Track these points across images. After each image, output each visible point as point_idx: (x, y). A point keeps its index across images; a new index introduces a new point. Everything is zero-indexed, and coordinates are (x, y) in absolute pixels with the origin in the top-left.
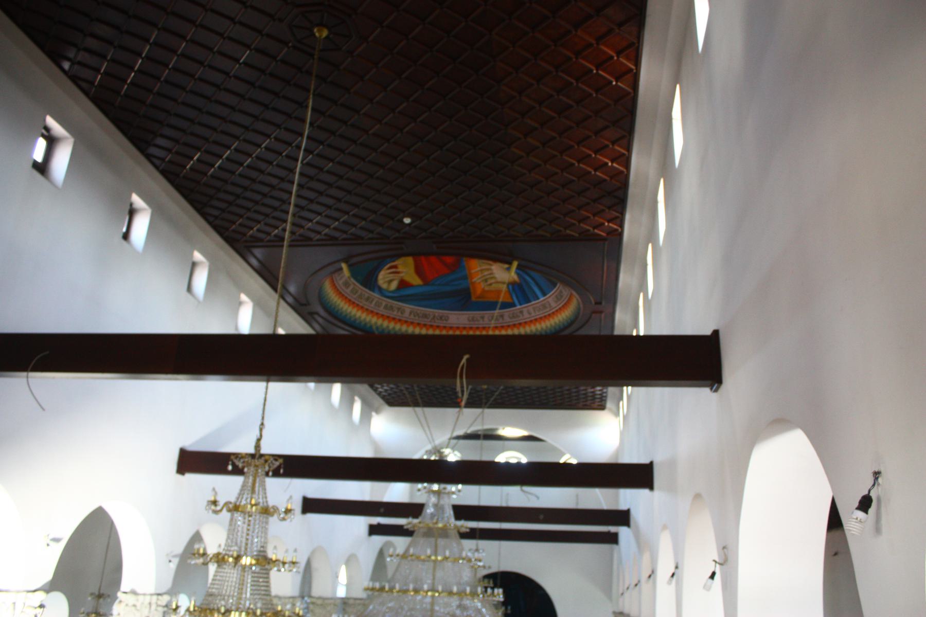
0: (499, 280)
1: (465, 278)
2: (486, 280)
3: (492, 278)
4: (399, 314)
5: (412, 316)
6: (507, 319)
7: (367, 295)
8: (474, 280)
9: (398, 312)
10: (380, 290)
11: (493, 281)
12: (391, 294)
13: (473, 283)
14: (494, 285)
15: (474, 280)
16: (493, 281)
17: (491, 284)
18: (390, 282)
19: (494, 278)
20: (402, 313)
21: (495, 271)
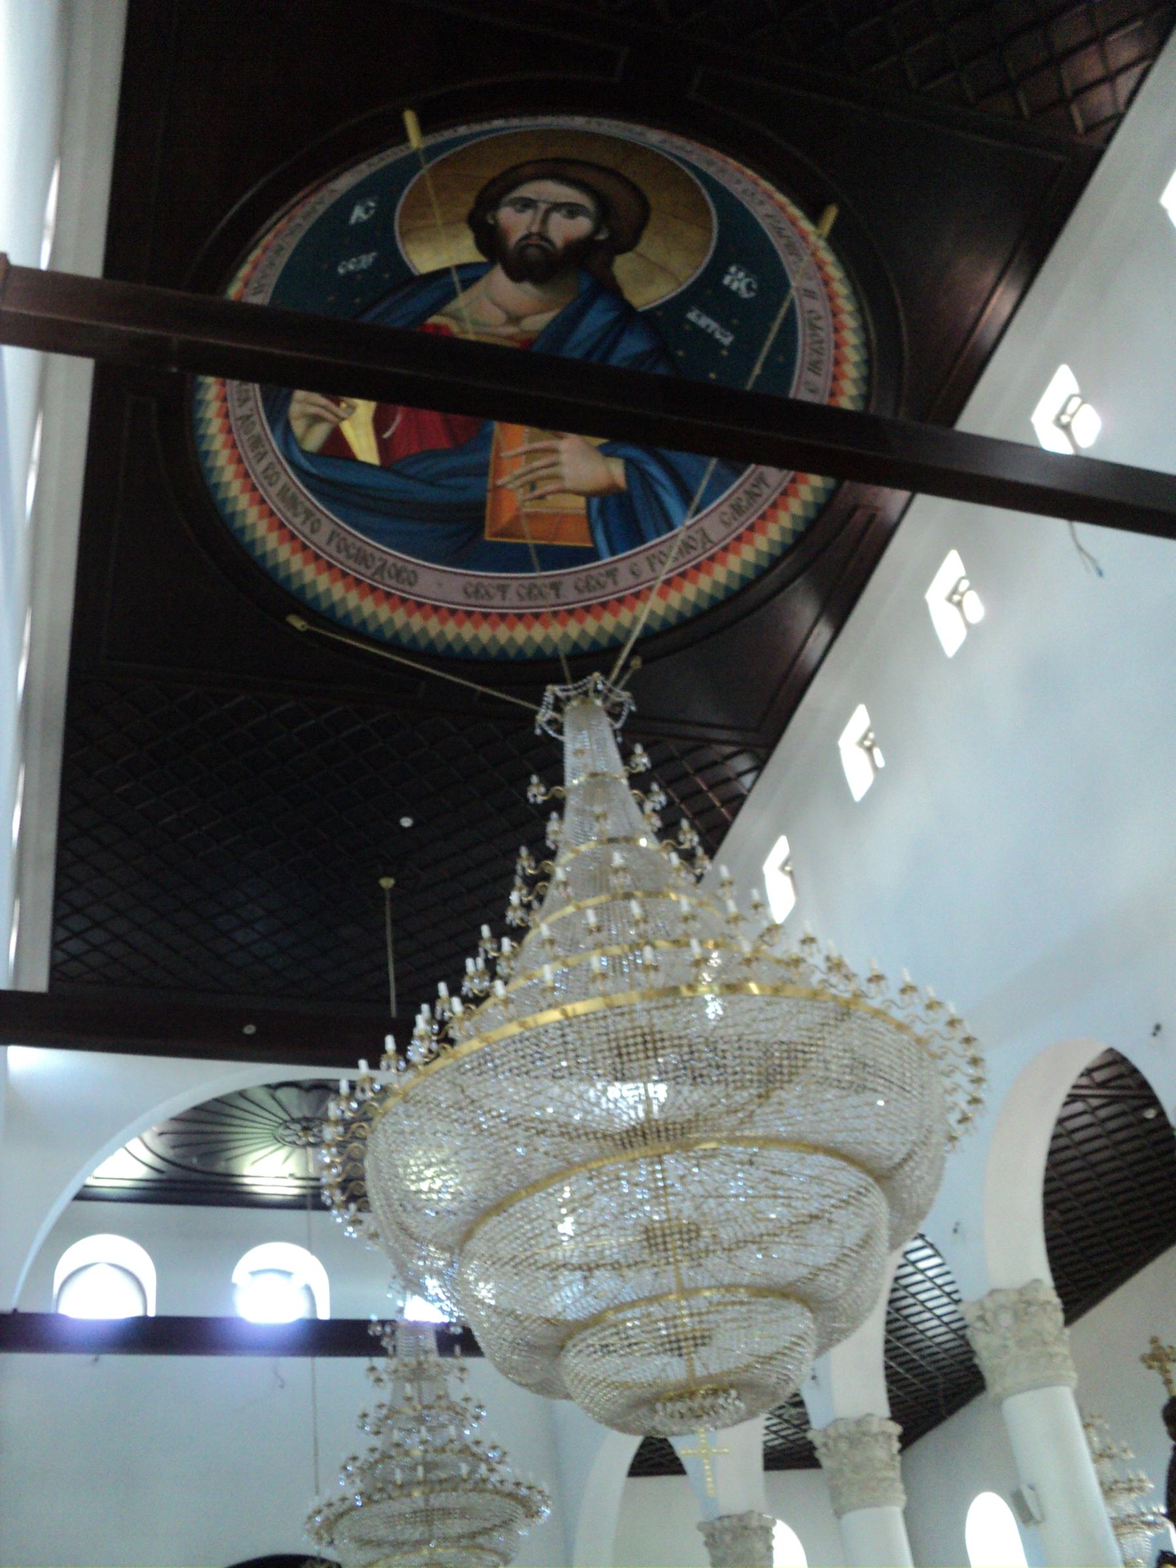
0: (568, 484)
1: (481, 471)
2: (533, 486)
4: (306, 529)
5: (332, 549)
6: (569, 594)
7: (258, 429)
8: (499, 482)
9: (304, 523)
10: (287, 436)
11: (551, 486)
12: (306, 464)
16: (551, 486)
17: (542, 497)
18: (316, 419)
19: (557, 477)
20: (313, 531)
21: (564, 457)
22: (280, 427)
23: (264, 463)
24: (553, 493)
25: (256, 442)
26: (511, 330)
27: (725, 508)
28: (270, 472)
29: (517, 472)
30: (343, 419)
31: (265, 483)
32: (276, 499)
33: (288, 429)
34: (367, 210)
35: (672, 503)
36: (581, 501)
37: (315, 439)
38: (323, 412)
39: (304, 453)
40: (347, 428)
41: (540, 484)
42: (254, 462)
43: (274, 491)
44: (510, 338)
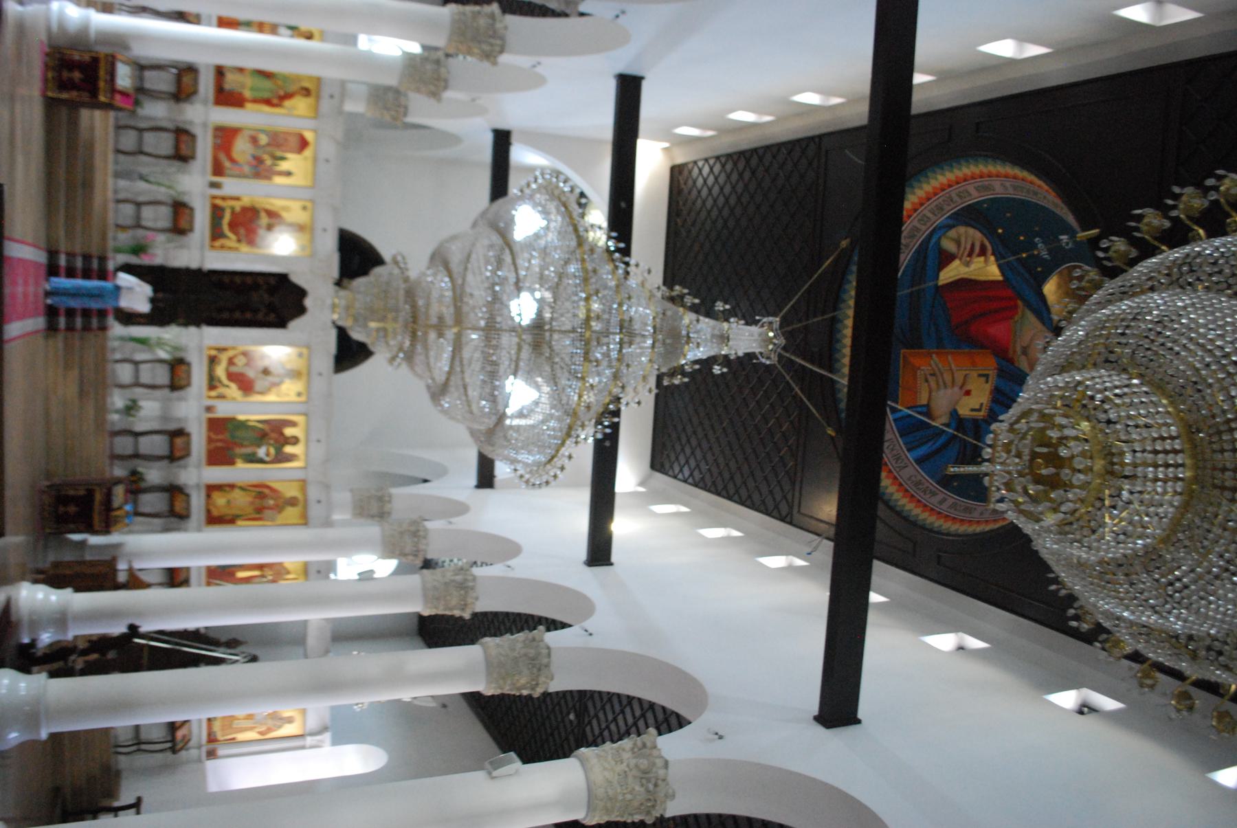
0: (933, 394)
1: (940, 345)
2: (933, 375)
3: (938, 384)
7: (947, 208)
8: (934, 356)
12: (934, 240)
13: (930, 355)
14: (926, 384)
15: (934, 356)
17: (927, 381)
18: (958, 243)
19: (938, 388)
21: (949, 391)
22: (951, 222)
23: (929, 215)
24: (929, 386)
25: (940, 208)
26: (1019, 349)
27: (919, 478)
28: (926, 219)
29: (940, 366)
30: (960, 259)
31: (919, 217)
32: (911, 226)
33: (951, 227)
34: (1067, 244)
35: (922, 451)
36: (925, 402)
37: (948, 245)
38: (963, 246)
39: (940, 238)
40: (956, 263)
41: (934, 378)
42: (929, 208)
43: (916, 223)
44: (1015, 352)
